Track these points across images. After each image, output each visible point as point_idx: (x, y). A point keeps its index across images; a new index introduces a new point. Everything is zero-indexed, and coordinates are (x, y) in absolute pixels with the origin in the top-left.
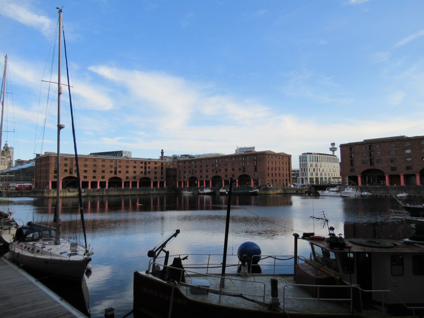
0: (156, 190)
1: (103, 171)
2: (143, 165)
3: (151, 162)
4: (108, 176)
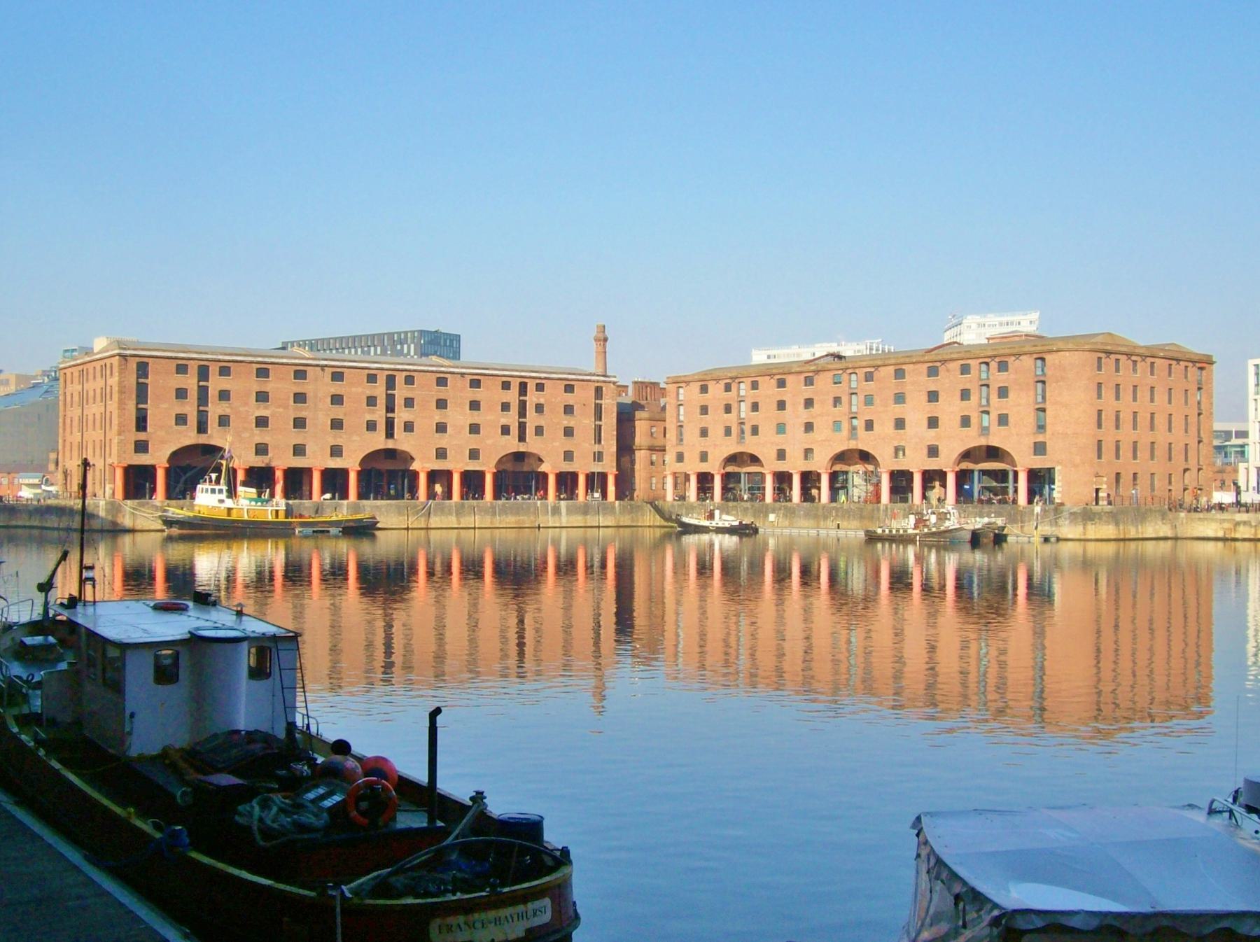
0: (570, 511)
2: (512, 396)
3: (547, 383)
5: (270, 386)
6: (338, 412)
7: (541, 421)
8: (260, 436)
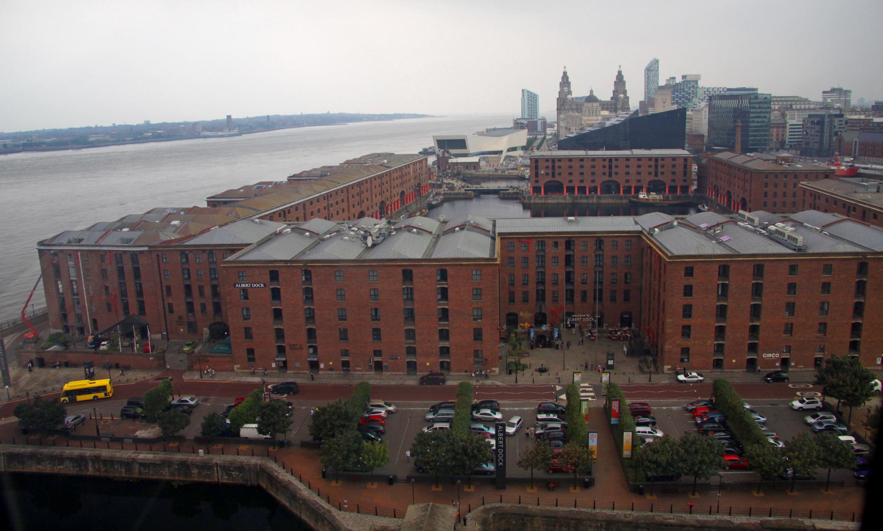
1: (593, 174)
4: (600, 180)
5: (572, 164)
6: (594, 170)
7: (663, 170)
8: (570, 178)
